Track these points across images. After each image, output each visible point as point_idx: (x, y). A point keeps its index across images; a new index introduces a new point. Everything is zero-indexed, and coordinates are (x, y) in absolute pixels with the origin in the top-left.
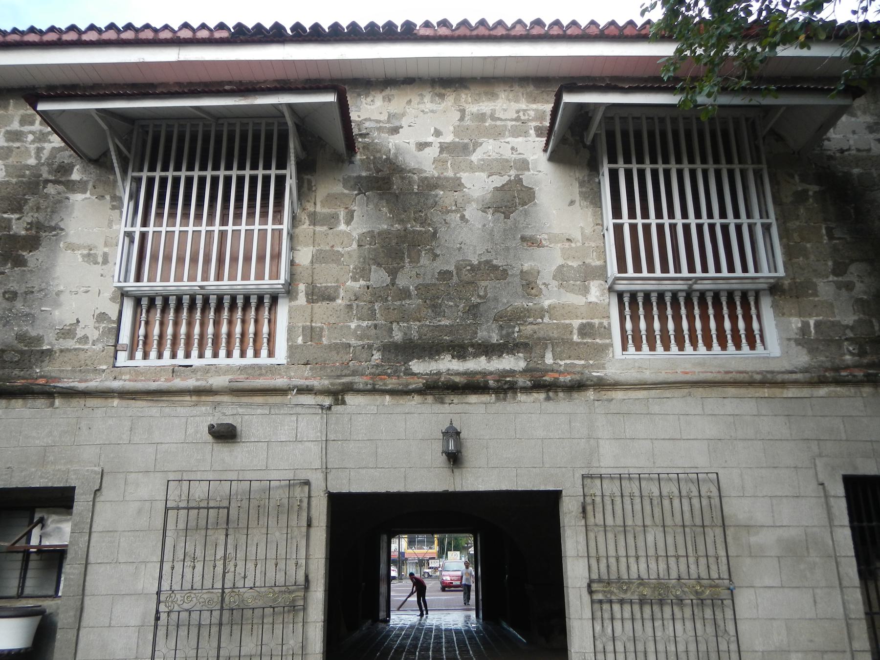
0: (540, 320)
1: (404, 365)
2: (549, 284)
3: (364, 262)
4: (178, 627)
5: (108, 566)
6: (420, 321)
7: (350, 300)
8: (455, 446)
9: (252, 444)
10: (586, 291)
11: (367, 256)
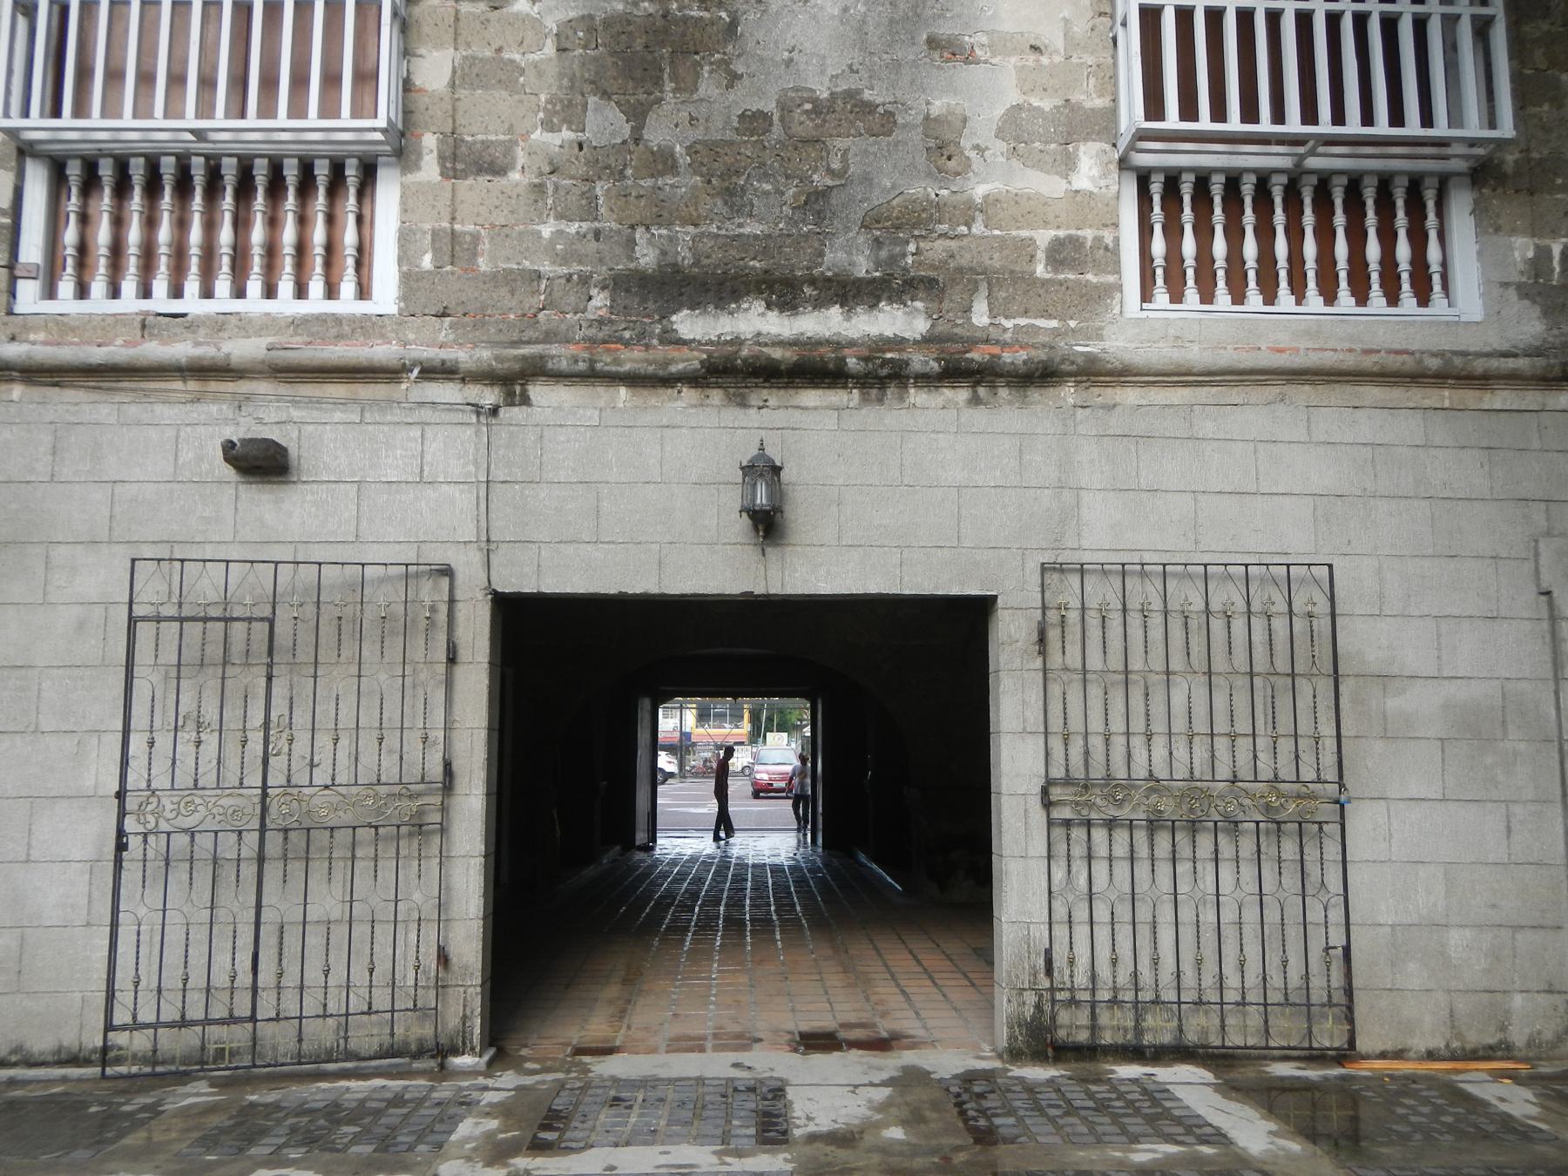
0: (963, 229)
1: (659, 322)
2: (987, 148)
3: (572, 88)
4: (167, 864)
5: (18, 738)
6: (696, 225)
7: (541, 174)
8: (771, 496)
9: (324, 486)
10: (1068, 165)
11: (578, 75)
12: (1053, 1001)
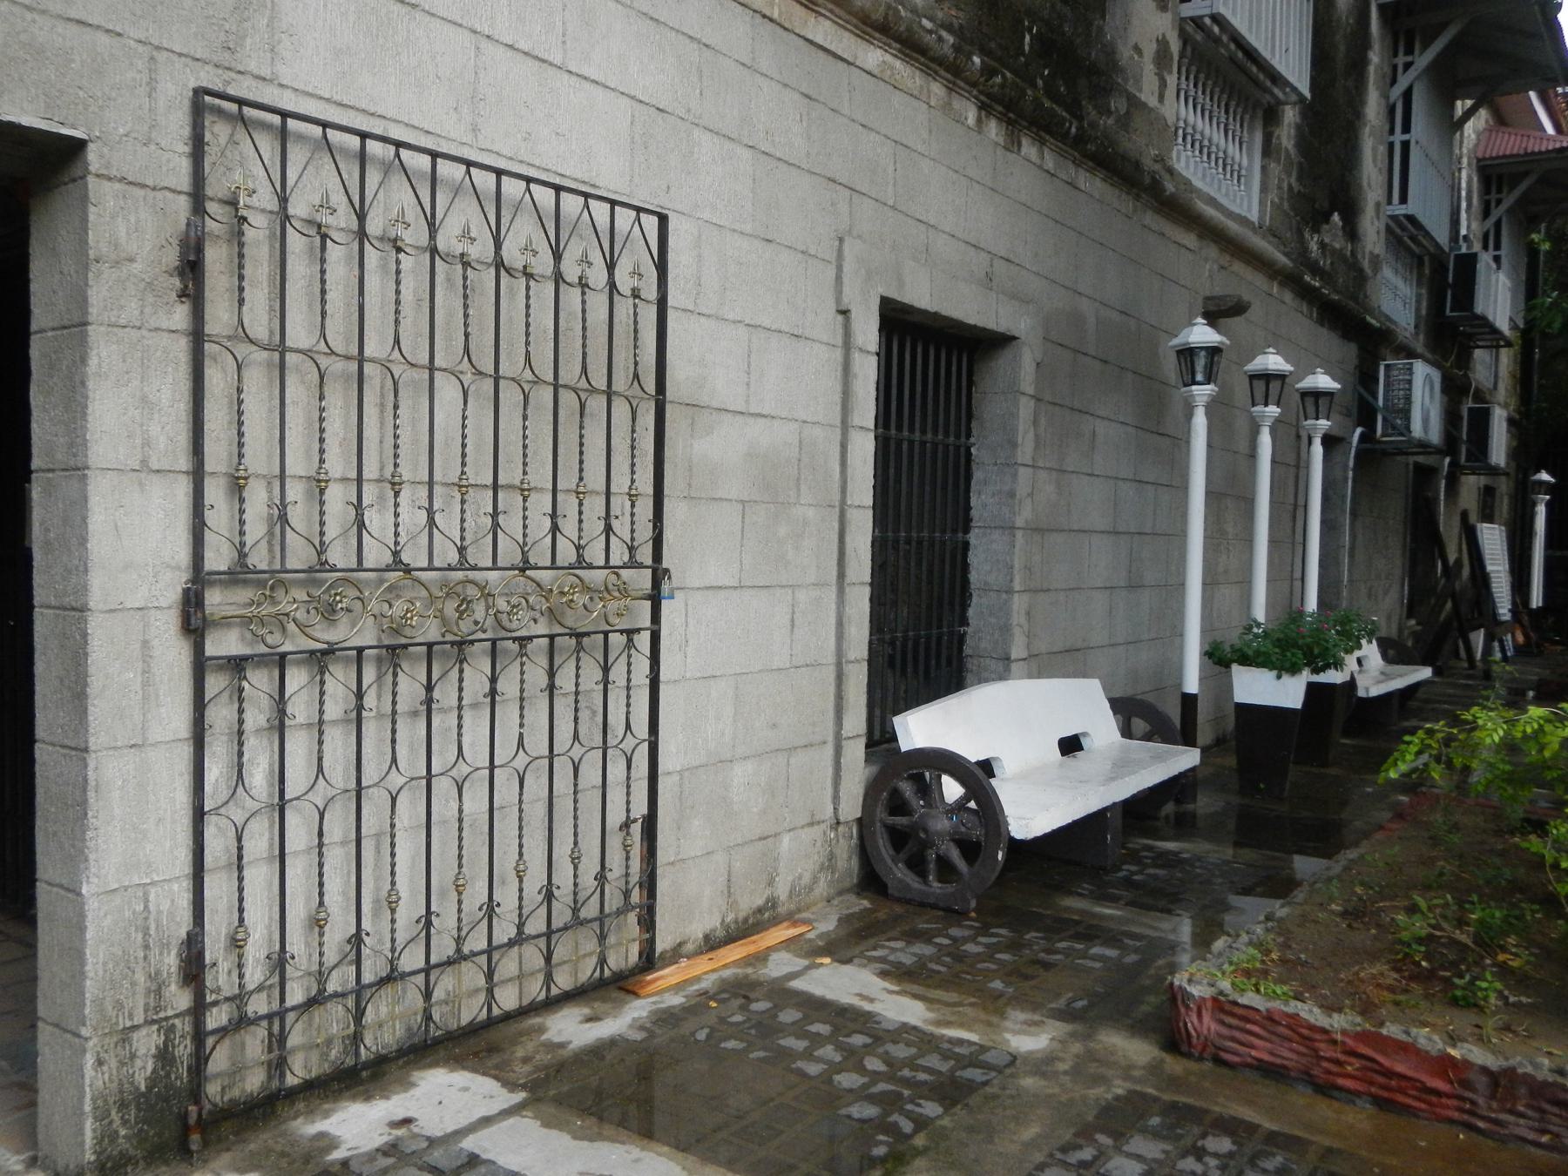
12: (199, 1035)
